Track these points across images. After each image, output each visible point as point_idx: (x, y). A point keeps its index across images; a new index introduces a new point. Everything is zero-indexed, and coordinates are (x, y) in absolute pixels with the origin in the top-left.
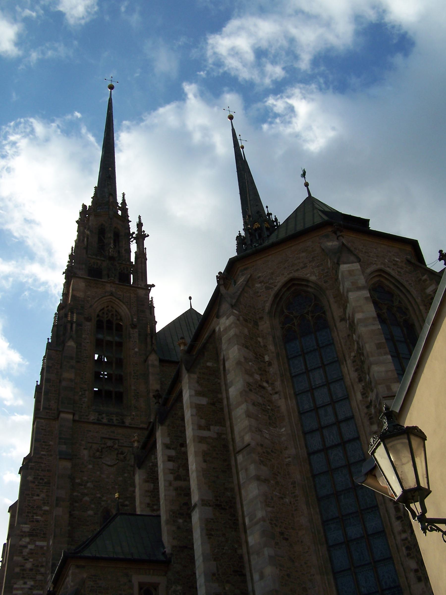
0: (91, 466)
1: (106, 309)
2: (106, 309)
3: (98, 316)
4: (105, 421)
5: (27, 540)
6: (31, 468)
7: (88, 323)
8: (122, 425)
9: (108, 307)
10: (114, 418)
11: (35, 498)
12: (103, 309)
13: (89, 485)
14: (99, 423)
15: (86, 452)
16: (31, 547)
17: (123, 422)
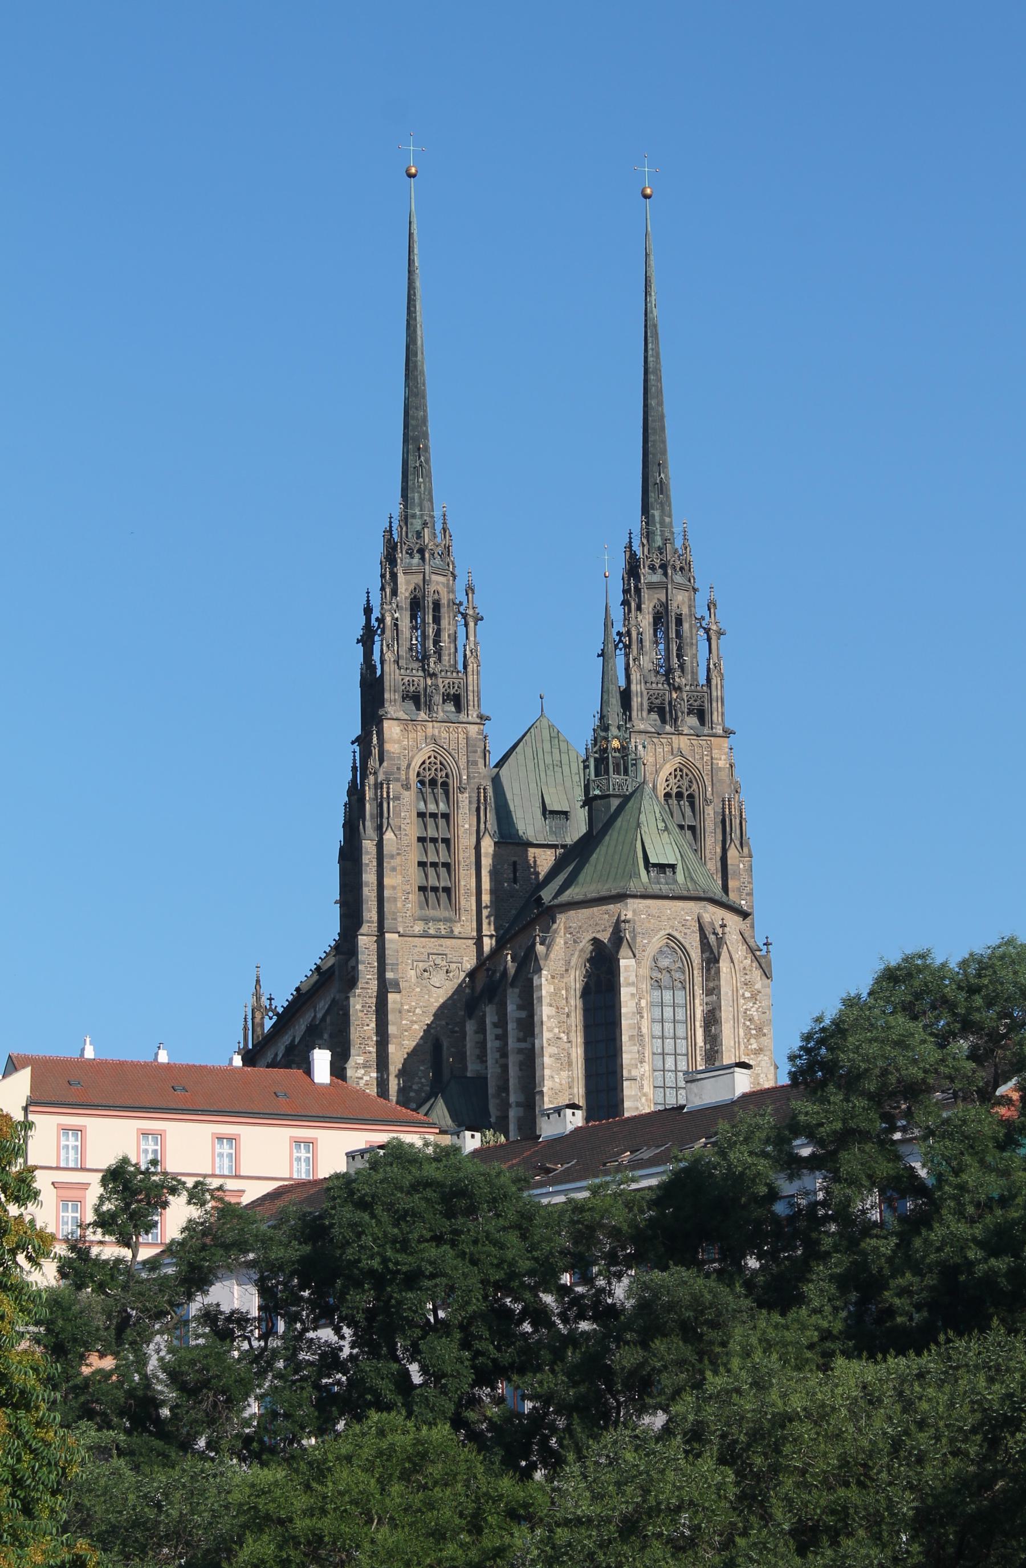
0: (418, 990)
1: (428, 762)
2: (428, 762)
3: (418, 774)
4: (432, 932)
5: (363, 1072)
6: (359, 996)
7: (406, 793)
8: (451, 936)
9: (429, 758)
10: (442, 927)
11: (366, 1028)
12: (424, 763)
13: (418, 1011)
14: (425, 935)
15: (413, 972)
16: (366, 1078)
17: (452, 931)
